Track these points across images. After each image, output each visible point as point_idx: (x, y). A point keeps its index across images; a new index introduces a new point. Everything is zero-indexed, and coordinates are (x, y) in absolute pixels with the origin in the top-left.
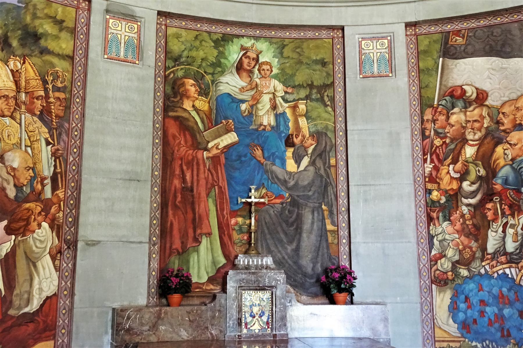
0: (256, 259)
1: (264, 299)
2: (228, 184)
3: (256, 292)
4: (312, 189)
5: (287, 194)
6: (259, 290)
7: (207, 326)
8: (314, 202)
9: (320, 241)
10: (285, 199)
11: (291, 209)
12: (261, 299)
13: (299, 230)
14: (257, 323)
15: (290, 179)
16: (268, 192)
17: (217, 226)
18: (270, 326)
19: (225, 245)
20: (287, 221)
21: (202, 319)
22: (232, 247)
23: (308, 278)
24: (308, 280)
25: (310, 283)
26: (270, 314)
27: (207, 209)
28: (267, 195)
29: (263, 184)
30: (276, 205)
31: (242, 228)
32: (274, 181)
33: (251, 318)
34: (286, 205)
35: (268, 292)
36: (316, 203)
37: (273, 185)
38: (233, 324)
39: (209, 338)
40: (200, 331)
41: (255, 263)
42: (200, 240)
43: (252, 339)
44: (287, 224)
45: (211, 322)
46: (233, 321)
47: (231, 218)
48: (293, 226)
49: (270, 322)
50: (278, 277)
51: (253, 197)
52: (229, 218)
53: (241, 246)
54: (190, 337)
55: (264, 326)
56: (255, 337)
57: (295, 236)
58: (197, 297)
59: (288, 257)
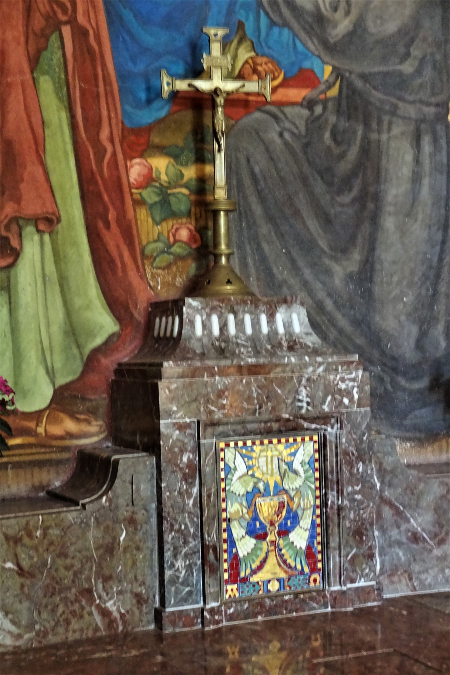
0: (251, 313)
1: (296, 466)
2: (110, 23)
3: (266, 442)
4: (416, 52)
5: (328, 69)
6: (280, 433)
7: (87, 586)
8: (422, 102)
9: (443, 242)
10: (322, 87)
11: (343, 124)
12: (284, 467)
13: (371, 206)
14: (272, 560)
15: (335, 9)
16: (259, 60)
17: (76, 190)
18: (319, 565)
19: (112, 262)
20: (329, 169)
21: (68, 561)
22: (137, 267)
23: (404, 374)
24: (402, 381)
25: (411, 393)
26: (318, 521)
27: (36, 120)
28: (255, 71)
29: (241, 25)
30: (288, 110)
31: (173, 200)
32: (281, 15)
33: (250, 542)
34: (325, 109)
35: (307, 438)
36: (428, 104)
37: (276, 30)
38: (189, 568)
39: (97, 629)
40: (61, 609)
41: (249, 330)
42: (14, 243)
43: (260, 618)
44: (330, 184)
45: (100, 566)
46: (186, 556)
47: (129, 157)
48: (350, 190)
49: (319, 548)
50: (343, 380)
51: (217, 75)
52: (120, 156)
53: (169, 266)
54: (26, 636)
55: (299, 567)
56: (271, 611)
57: (357, 226)
58: (17, 466)
59: (335, 303)
